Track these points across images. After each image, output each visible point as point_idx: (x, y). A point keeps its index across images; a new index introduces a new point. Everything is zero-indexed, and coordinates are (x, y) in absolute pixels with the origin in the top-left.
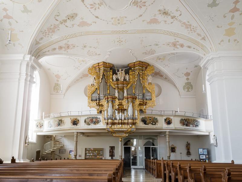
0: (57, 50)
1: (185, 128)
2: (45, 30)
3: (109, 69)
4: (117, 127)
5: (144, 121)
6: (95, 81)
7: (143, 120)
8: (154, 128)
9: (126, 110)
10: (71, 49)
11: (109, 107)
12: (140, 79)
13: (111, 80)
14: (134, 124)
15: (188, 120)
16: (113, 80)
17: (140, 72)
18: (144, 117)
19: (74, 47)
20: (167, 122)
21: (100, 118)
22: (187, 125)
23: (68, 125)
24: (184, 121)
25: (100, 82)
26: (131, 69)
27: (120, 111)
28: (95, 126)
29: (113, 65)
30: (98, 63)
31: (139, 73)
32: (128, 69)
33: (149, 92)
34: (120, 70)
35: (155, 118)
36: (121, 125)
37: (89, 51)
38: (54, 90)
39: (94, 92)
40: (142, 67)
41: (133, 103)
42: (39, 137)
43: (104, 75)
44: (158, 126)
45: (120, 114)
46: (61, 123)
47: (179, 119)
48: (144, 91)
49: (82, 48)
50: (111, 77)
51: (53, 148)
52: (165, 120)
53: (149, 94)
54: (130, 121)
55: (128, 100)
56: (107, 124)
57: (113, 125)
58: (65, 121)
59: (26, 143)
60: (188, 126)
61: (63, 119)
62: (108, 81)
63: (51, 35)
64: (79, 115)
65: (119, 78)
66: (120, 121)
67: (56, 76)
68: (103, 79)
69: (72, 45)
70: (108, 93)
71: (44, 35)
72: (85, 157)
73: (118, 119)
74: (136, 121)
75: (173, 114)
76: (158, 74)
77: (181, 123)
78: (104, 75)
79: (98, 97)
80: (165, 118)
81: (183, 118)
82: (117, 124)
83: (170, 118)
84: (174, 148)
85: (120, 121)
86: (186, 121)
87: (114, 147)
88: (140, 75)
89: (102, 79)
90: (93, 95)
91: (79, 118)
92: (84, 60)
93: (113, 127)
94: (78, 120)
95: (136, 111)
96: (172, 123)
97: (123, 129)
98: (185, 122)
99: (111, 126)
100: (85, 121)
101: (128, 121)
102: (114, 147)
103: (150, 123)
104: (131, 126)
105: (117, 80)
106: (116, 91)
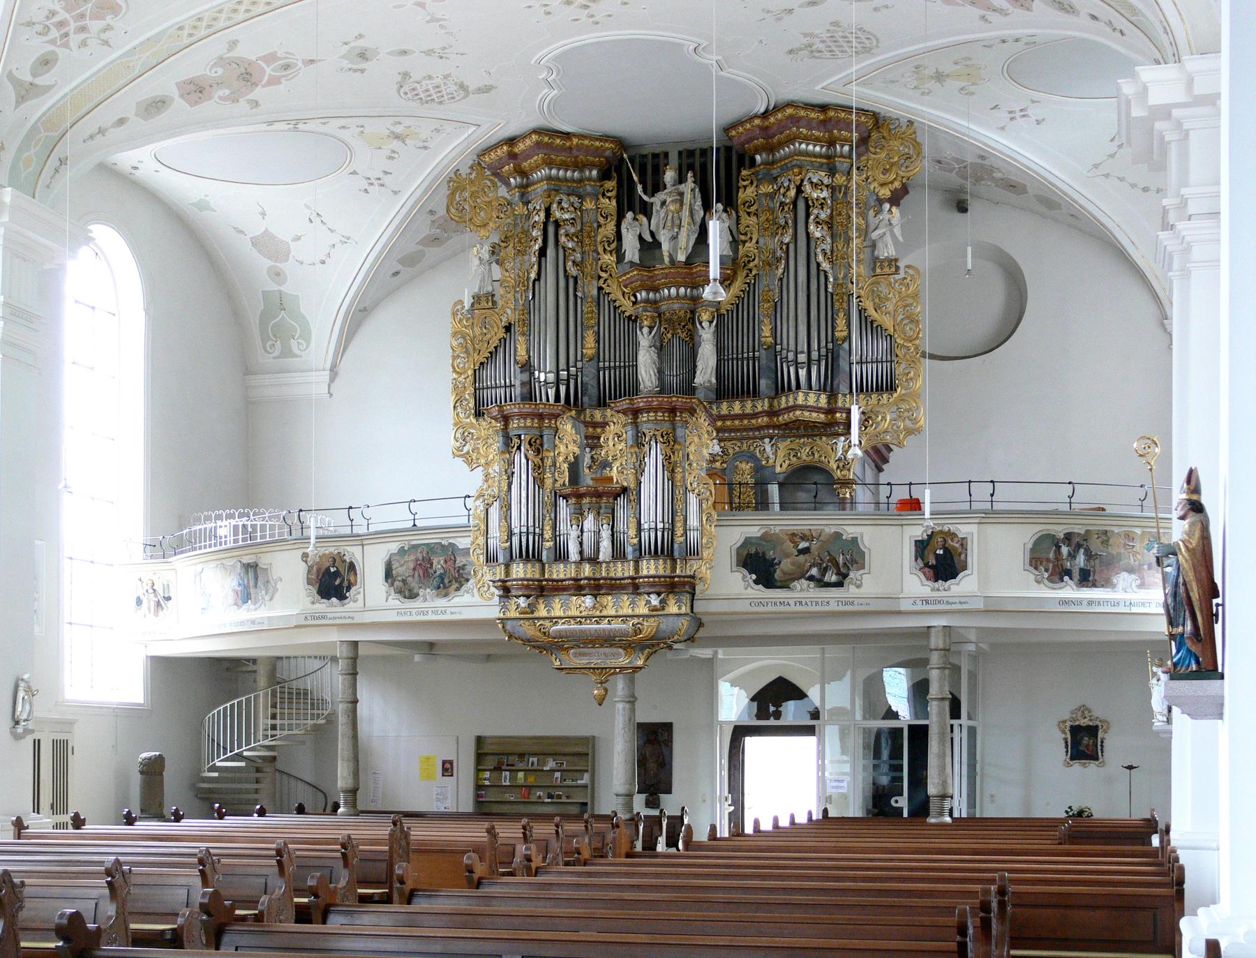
0: (179, 103)
1: (1065, 602)
2: (53, 13)
3: (594, 173)
4: (566, 612)
5: (759, 564)
6: (497, 272)
7: (749, 555)
8: (833, 607)
9: (625, 490)
10: (274, 81)
11: (515, 480)
12: (808, 234)
13: (609, 259)
14: (672, 586)
15: (1095, 545)
16: (620, 257)
17: (807, 188)
18: (755, 532)
19: (286, 67)
20: (932, 561)
21: (466, 552)
22: (1086, 579)
23: (291, 597)
24: (1065, 550)
25: (533, 276)
26: (753, 163)
27: (586, 501)
28: (442, 602)
29: (621, 143)
30: (511, 141)
31: (799, 190)
32: (725, 166)
33: (869, 325)
34: (669, 176)
35: (838, 535)
36: (589, 601)
37: (406, 75)
38: (264, 340)
39: (493, 355)
40: (831, 143)
41: (671, 440)
42: (168, 671)
43: (557, 225)
44: (867, 587)
45: (589, 523)
46: (256, 586)
47: (1025, 535)
48: (841, 322)
49: (345, 64)
50: (610, 228)
51: (266, 737)
52: (922, 547)
53: (883, 345)
54: (645, 572)
55: (635, 424)
56: (506, 591)
57: (541, 601)
58: (275, 573)
59: (17, 723)
60: (1094, 585)
61: (264, 561)
62: (589, 260)
63: (104, 30)
65: (664, 237)
66: (587, 570)
67: (255, 242)
68: (550, 252)
69: (271, 58)
70: (589, 352)
71: (53, 42)
72: (478, 796)
73: (574, 555)
74: (694, 566)
75: (975, 506)
76: (967, 187)
77: (1036, 561)
78: (557, 225)
79: (518, 383)
80: (919, 532)
81: (1060, 531)
82: (565, 589)
83: (953, 535)
84: (1092, 731)
85: (587, 570)
86: (1079, 546)
87: (668, 727)
88: (808, 207)
89: (542, 252)
90: (488, 375)
92: (399, 129)
93: (542, 611)
95: (693, 500)
96: (965, 568)
97: (604, 625)
98: (1072, 556)
99: (532, 608)
100: (389, 574)
101: (637, 569)
102: (668, 727)
103: (802, 576)
104: (655, 600)
105: (650, 246)
106: (645, 339)
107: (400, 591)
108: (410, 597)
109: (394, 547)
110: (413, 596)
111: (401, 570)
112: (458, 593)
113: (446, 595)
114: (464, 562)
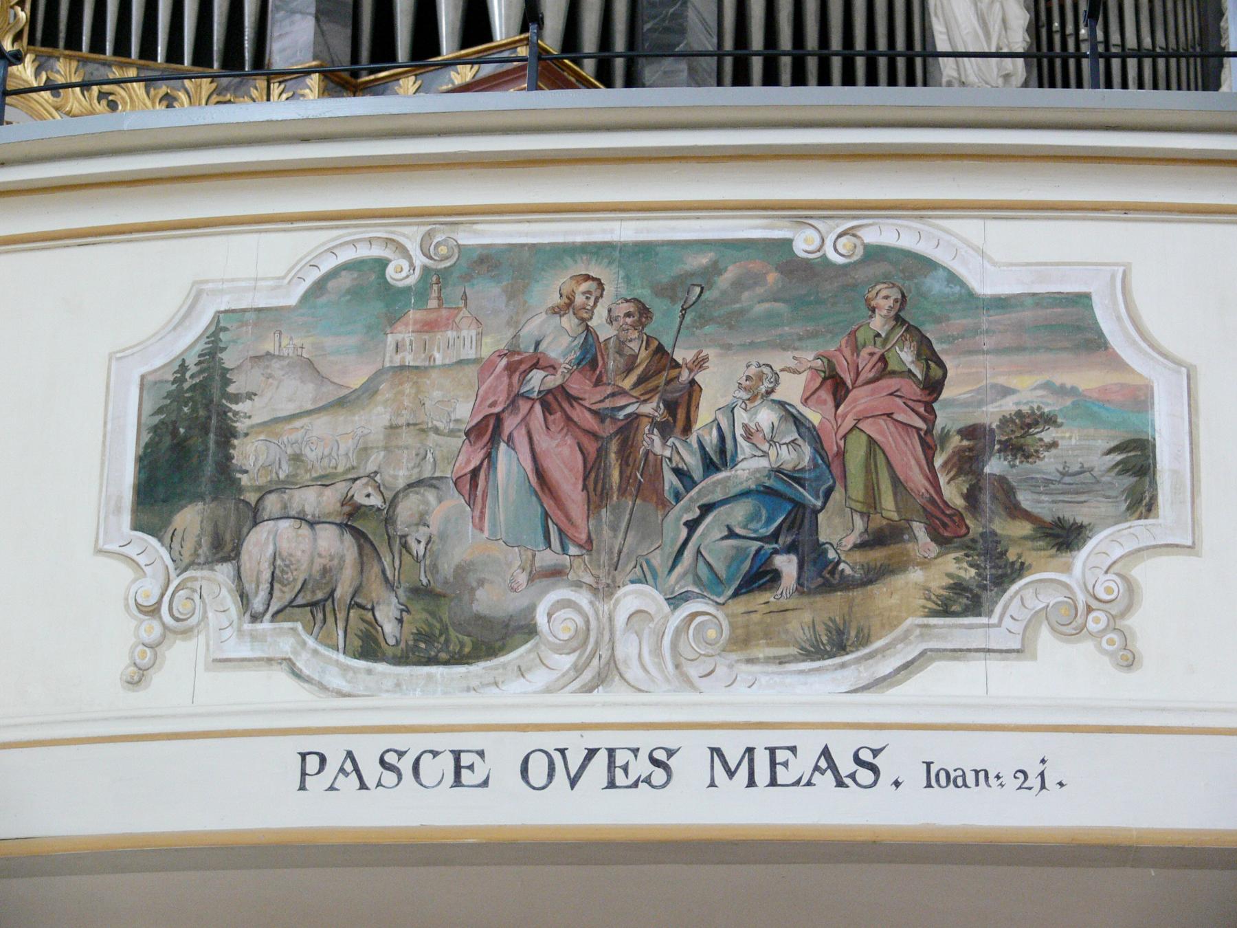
21: (1066, 324)
107: (313, 603)
108: (426, 649)
111: (331, 439)
113: (836, 643)
114: (1024, 388)
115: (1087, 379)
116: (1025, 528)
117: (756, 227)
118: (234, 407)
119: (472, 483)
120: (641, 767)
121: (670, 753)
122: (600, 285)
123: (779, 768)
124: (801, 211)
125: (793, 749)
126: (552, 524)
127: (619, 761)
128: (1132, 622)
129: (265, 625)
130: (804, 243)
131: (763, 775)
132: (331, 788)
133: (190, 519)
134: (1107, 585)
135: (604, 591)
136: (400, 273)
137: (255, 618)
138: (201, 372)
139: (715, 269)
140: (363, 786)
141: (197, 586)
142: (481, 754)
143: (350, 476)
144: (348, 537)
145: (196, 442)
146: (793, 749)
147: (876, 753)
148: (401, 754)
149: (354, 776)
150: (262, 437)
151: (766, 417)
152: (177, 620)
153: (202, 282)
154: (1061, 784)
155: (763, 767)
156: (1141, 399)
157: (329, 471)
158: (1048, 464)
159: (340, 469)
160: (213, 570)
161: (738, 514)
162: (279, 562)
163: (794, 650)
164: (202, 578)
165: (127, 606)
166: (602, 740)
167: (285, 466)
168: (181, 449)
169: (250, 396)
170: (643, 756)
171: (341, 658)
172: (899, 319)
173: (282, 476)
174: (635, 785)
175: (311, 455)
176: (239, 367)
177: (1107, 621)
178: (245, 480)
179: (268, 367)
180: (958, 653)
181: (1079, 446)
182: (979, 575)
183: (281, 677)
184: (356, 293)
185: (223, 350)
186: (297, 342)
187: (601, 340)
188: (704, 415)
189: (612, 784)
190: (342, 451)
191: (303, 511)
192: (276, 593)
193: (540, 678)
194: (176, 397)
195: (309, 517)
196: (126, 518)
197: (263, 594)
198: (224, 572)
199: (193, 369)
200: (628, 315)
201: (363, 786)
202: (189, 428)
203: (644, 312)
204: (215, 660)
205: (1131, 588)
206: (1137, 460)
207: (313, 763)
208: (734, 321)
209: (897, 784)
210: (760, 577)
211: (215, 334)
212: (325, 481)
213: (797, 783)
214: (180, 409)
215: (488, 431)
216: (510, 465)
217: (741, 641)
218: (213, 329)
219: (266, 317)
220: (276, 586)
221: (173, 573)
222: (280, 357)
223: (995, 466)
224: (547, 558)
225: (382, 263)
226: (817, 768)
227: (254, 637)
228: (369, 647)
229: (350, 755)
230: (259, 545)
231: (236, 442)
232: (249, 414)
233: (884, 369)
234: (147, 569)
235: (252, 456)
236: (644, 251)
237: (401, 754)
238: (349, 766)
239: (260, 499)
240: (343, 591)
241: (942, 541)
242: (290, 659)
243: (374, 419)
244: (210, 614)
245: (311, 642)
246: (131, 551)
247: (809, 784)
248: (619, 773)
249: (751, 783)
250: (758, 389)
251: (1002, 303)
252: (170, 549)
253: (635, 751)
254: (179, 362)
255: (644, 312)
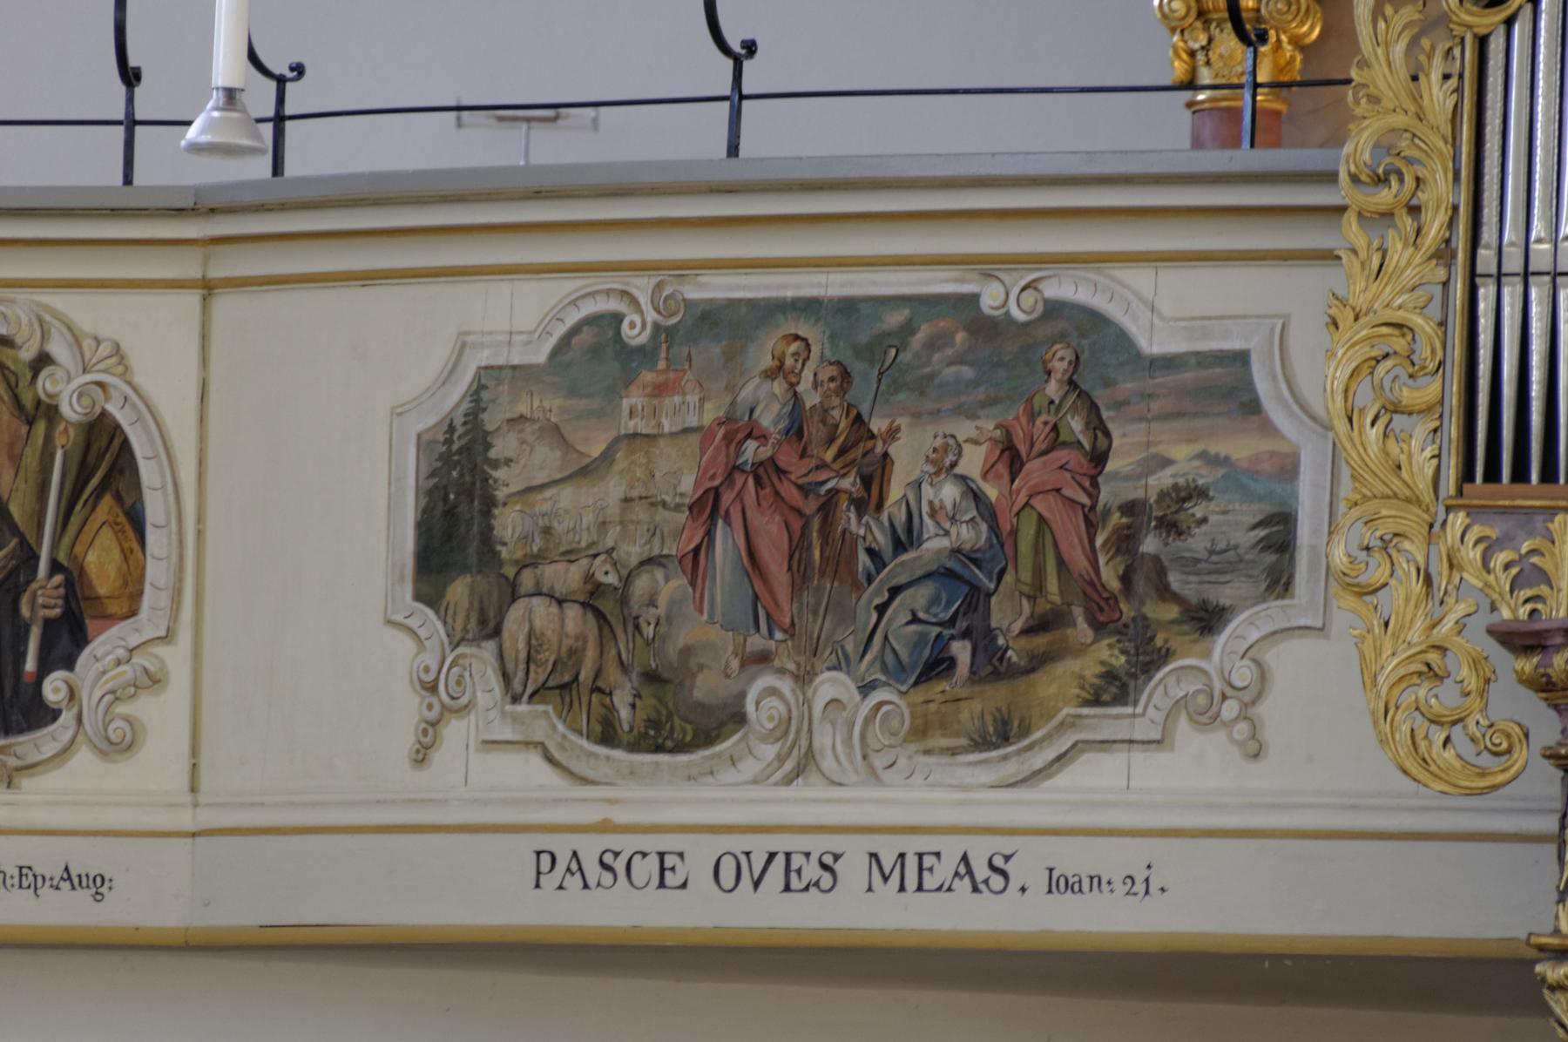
28: (951, 795)
64: (162, 164)
91: (136, 345)
94: (105, 465)
100: (455, 534)
107: (556, 684)
108: (656, 737)
109: (518, 317)
110: (680, 723)
112: (1110, 722)
113: (1002, 733)
114: (1183, 458)
115: (1241, 447)
116: (1171, 612)
117: (947, 281)
118: (495, 474)
119: (695, 562)
120: (812, 871)
121: (837, 857)
122: (808, 345)
123: (926, 874)
124: (987, 265)
125: (938, 855)
126: (759, 611)
127: (794, 866)
128: (1262, 709)
129: (523, 708)
130: (991, 298)
131: (911, 882)
132: (561, 887)
133: (459, 591)
134: (1243, 674)
135: (803, 679)
136: (635, 333)
137: (515, 699)
138: (466, 433)
139: (908, 329)
140: (586, 886)
141: (466, 662)
142: (681, 855)
143: (591, 552)
144: (590, 616)
145: (463, 508)
146: (938, 855)
147: (1007, 858)
148: (617, 854)
149: (578, 875)
150: (518, 507)
151: (949, 492)
152: (453, 698)
153: (468, 333)
154: (1163, 890)
155: (904, 872)
156: (1288, 469)
157: (574, 546)
158: (1197, 543)
159: (583, 544)
160: (479, 646)
161: (919, 597)
162: (533, 641)
163: (964, 741)
164: (472, 656)
165: (412, 682)
166: (781, 843)
167: (537, 540)
168: (450, 514)
169: (508, 462)
170: (814, 858)
171: (584, 743)
172: (1072, 384)
173: (535, 549)
174: (806, 889)
175: (558, 528)
176: (498, 429)
177: (1238, 711)
178: (504, 552)
179: (521, 431)
180: (1105, 744)
181: (1229, 523)
182: (1128, 662)
183: (535, 760)
184: (595, 351)
185: (484, 410)
186: (547, 404)
187: (808, 407)
188: (895, 492)
189: (787, 888)
190: (584, 525)
191: (552, 588)
192: (532, 675)
193: (749, 768)
194: (446, 459)
195: (557, 595)
196: (408, 589)
197: (521, 675)
198: (490, 646)
199: (460, 430)
200: (832, 379)
201: (586, 886)
202: (457, 495)
203: (845, 376)
204: (485, 742)
205: (1263, 673)
206: (1279, 534)
207: (546, 860)
208: (922, 387)
209: (1023, 889)
210: (937, 666)
211: (477, 392)
212: (570, 555)
213: (939, 889)
214: (449, 473)
215: (708, 506)
216: (726, 544)
217: (920, 731)
218: (475, 387)
219: (520, 374)
220: (532, 667)
221: (448, 650)
222: (532, 420)
223: (1150, 544)
224: (757, 642)
225: (618, 318)
226: (957, 874)
227: (515, 719)
228: (608, 735)
229: (575, 854)
230: (514, 622)
231: (496, 512)
232: (507, 481)
233: (1056, 440)
234: (427, 643)
235: (509, 524)
236: (848, 307)
237: (617, 854)
238: (574, 867)
239: (518, 573)
240: (586, 674)
241: (1099, 627)
242: (542, 744)
243: (613, 489)
244: (479, 694)
245: (561, 727)
246: (413, 623)
247: (949, 889)
248: (794, 876)
249: (902, 888)
250: (943, 464)
251: (1169, 363)
252: (445, 623)
253: (807, 855)
254: (447, 422)
255: (845, 376)
